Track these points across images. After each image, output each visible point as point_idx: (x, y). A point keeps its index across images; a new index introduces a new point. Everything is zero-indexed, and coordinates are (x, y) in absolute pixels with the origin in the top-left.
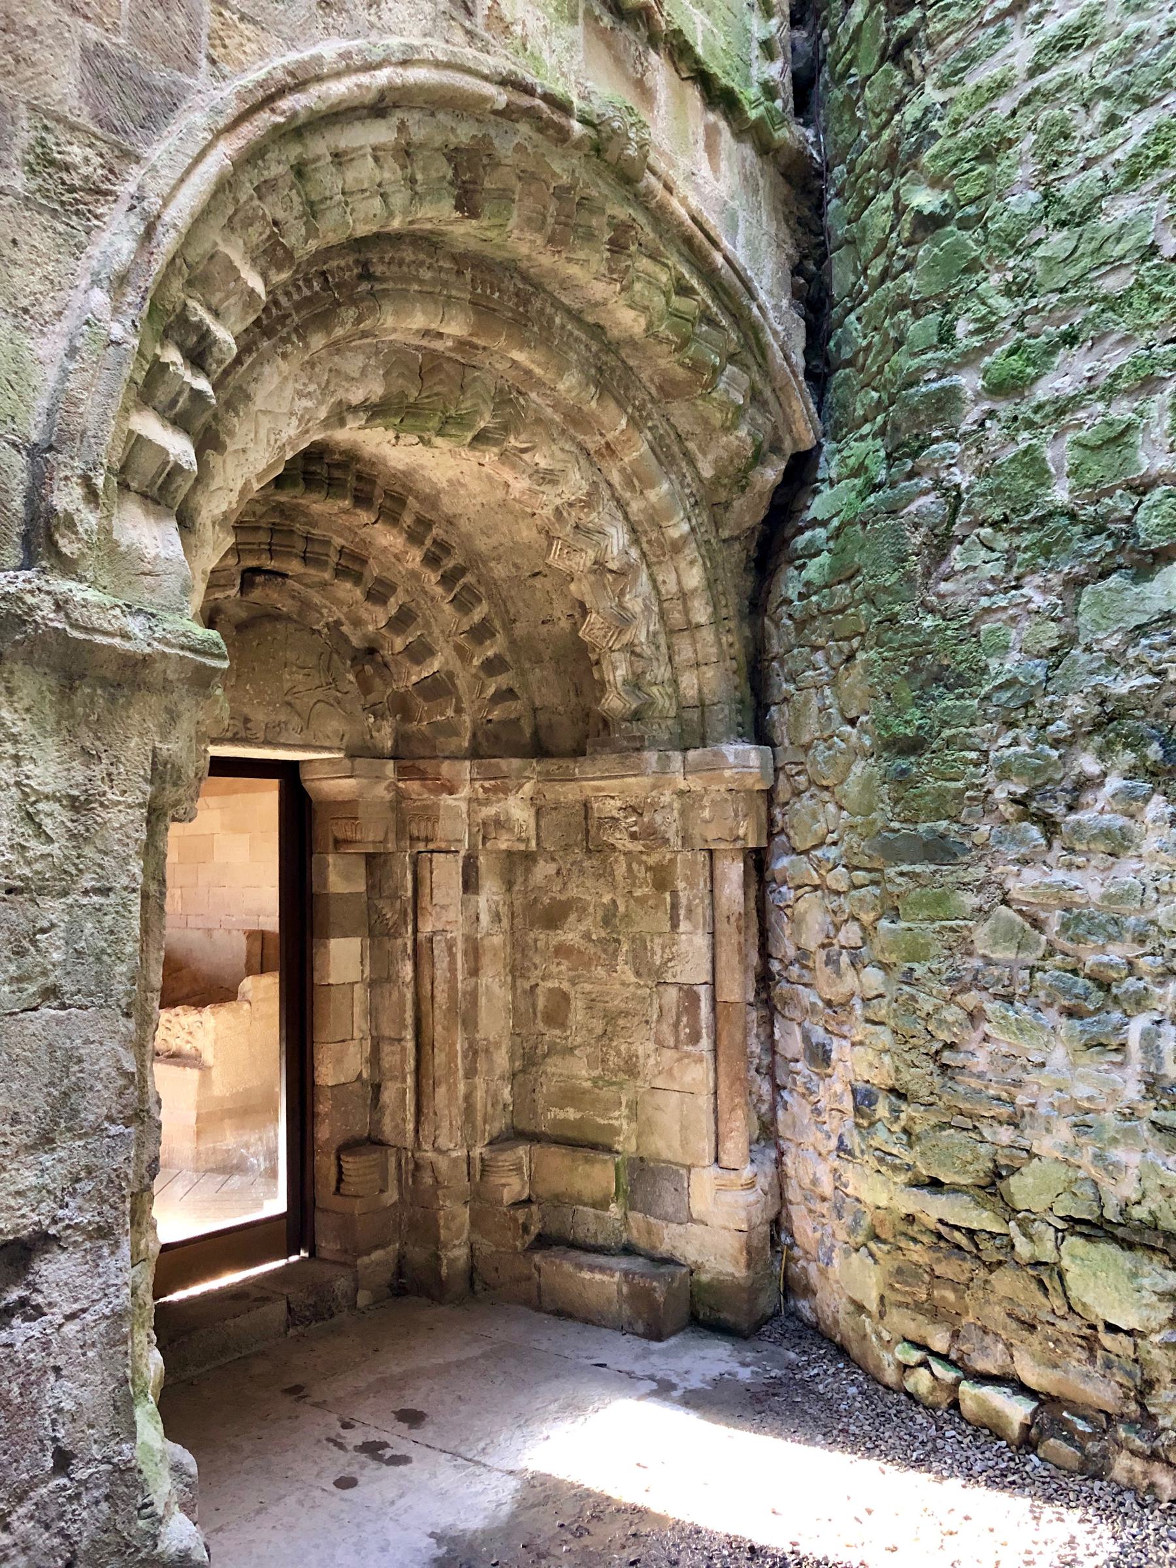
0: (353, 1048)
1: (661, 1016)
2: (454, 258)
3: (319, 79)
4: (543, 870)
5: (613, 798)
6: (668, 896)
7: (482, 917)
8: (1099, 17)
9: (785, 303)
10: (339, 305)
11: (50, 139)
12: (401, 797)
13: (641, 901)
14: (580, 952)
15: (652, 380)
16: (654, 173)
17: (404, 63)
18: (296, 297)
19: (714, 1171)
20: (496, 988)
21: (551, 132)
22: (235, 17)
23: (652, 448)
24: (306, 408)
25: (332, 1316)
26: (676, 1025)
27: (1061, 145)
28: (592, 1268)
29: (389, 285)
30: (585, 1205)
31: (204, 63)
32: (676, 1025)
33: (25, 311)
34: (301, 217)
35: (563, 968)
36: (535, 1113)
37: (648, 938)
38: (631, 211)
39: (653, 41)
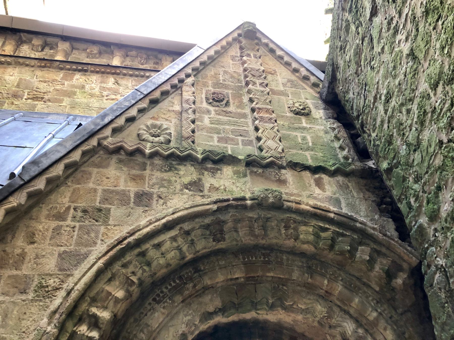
2: (233, 253)
3: (140, 230)
8: (390, 87)
9: (376, 217)
10: (186, 284)
11: (43, 281)
15: (334, 263)
16: (289, 201)
17: (173, 213)
18: (169, 287)
21: (240, 207)
22: (112, 227)
23: (346, 287)
24: (189, 320)
27: (402, 127)
29: (207, 271)
31: (99, 242)
33: (24, 332)
34: (140, 268)
38: (288, 215)
39: (281, 167)
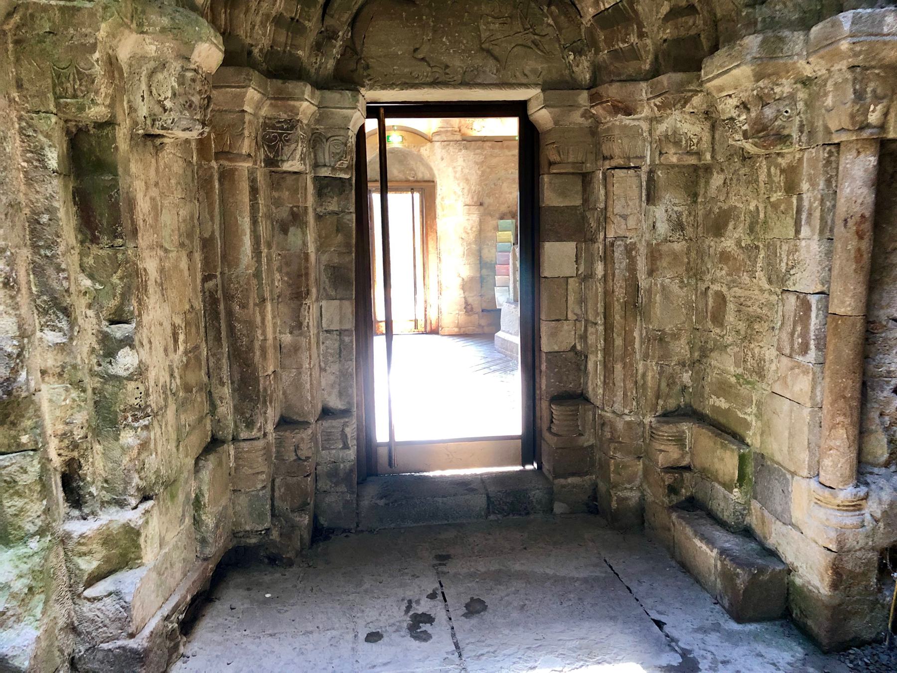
0: (566, 326)
1: (782, 324)
4: (717, 180)
5: (730, 96)
6: (794, 200)
7: (658, 225)
12: (598, 122)
13: (775, 206)
14: (735, 259)
19: (813, 484)
20: (675, 287)
25: (528, 514)
26: (792, 334)
28: (703, 538)
30: (720, 483)
32: (792, 334)
35: (724, 272)
36: (703, 396)
37: (778, 243)
